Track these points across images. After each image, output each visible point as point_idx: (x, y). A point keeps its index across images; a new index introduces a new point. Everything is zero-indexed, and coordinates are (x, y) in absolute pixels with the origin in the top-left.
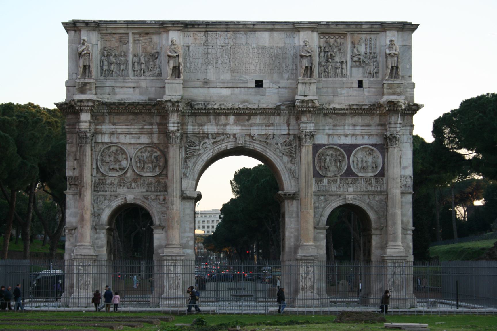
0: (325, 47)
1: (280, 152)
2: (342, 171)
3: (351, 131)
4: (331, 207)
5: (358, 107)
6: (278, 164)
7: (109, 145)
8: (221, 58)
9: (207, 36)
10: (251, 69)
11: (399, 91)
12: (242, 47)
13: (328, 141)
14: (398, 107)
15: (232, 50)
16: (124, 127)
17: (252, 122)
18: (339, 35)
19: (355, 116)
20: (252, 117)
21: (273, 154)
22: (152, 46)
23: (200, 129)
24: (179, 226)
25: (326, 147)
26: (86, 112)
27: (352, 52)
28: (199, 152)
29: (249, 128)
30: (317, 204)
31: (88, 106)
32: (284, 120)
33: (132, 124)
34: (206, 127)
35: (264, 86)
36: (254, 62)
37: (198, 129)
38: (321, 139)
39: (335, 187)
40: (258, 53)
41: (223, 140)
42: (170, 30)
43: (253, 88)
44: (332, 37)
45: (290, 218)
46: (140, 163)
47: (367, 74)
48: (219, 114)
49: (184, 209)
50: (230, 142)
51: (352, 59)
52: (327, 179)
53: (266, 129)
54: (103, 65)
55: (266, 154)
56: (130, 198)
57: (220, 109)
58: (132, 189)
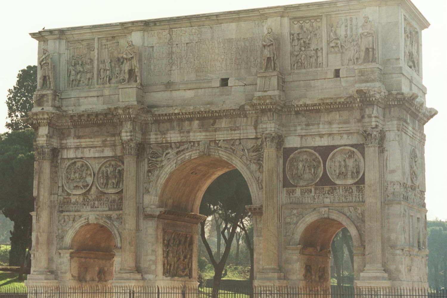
0: (298, 34)
1: (247, 159)
2: (317, 179)
3: (326, 130)
4: (304, 222)
5: (332, 101)
6: (245, 174)
7: (73, 161)
8: (185, 57)
9: (171, 34)
10: (216, 66)
11: (372, 77)
12: (207, 43)
13: (301, 143)
14: (370, 97)
15: (196, 46)
16: (88, 140)
17: (217, 126)
18: (315, 18)
19: (332, 111)
20: (217, 120)
21: (239, 162)
22: (119, 49)
23: (163, 138)
24: (132, 247)
25: (299, 150)
26: (44, 126)
27: (329, 37)
28: (162, 164)
29: (214, 133)
30: (289, 220)
31: (44, 119)
32: (251, 122)
33: (95, 136)
34: (169, 135)
35: (229, 85)
36: (219, 58)
37: (160, 138)
38: (293, 142)
39: (309, 199)
40: (224, 47)
41: (187, 149)
42: (133, 31)
43: (218, 87)
44: (308, 21)
45: (258, 236)
46: (103, 179)
47: (348, 61)
48: (181, 120)
49: (146, 229)
50: (193, 150)
51: (328, 44)
52: (300, 190)
53: (232, 134)
54: (70, 75)
55: (232, 163)
56: (92, 219)
57: (181, 113)
58: (96, 208)
